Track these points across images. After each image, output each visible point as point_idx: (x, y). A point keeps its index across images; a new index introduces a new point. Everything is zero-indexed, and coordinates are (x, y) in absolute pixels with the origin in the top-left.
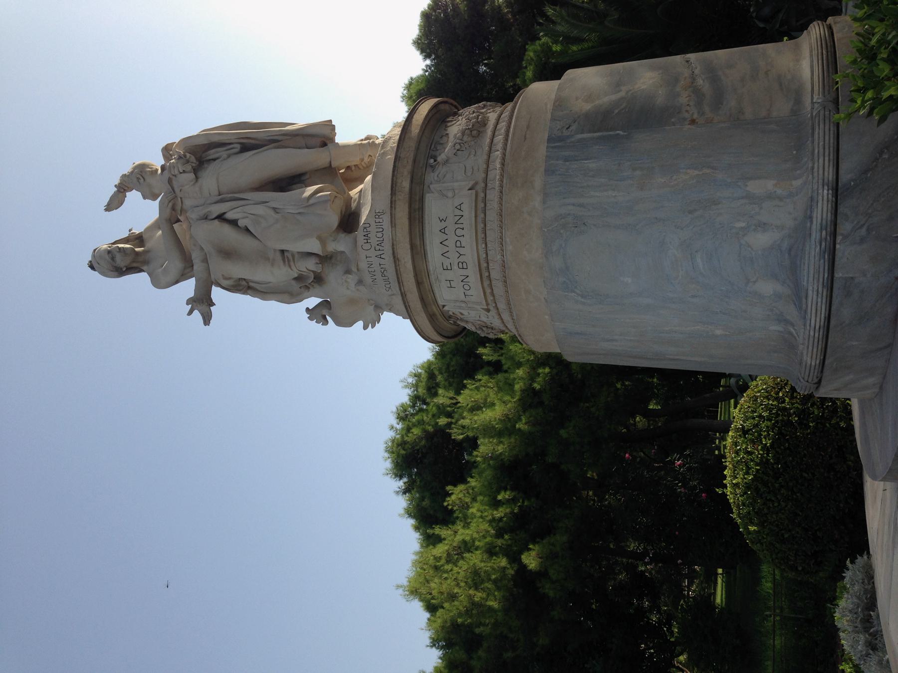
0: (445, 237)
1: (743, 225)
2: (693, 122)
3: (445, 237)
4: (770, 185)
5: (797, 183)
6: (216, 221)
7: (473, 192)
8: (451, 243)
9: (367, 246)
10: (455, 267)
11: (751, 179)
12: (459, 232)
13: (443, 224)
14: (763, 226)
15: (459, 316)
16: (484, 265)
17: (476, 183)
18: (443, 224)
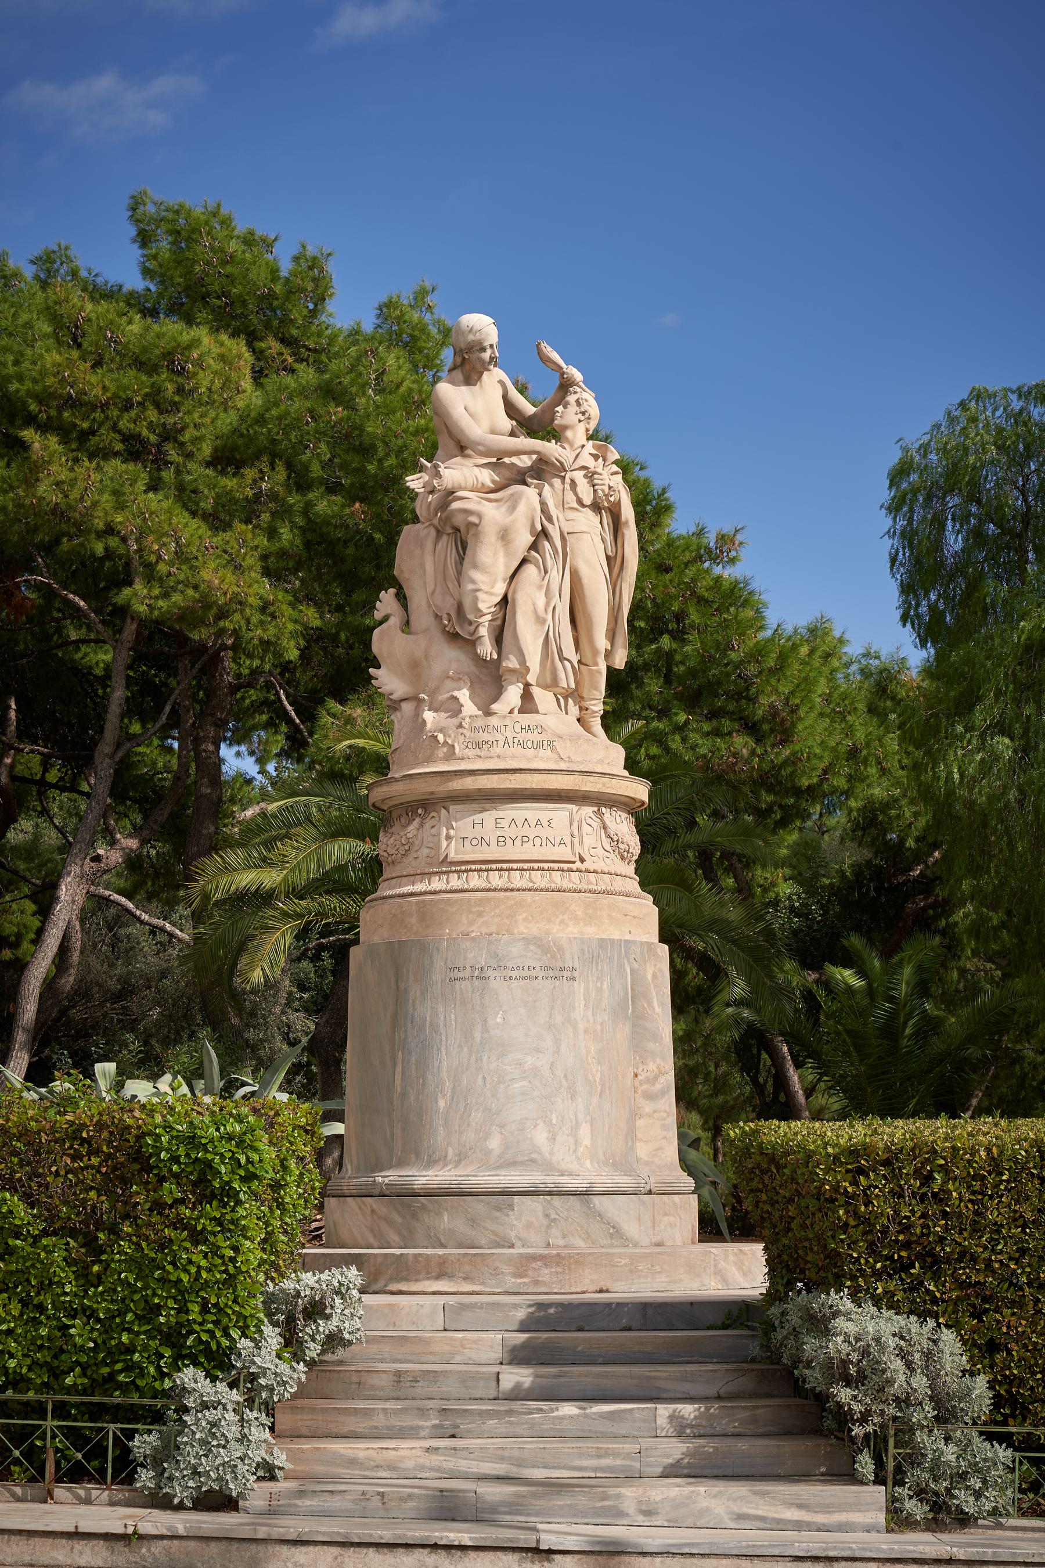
0: (533, 825)
1: (554, 1121)
2: (636, 1076)
3: (533, 825)
4: (587, 1142)
5: (588, 1164)
6: (539, 528)
7: (577, 859)
8: (526, 831)
9: (518, 729)
10: (499, 833)
11: (592, 1125)
12: (538, 841)
13: (545, 824)
14: (553, 1139)
15: (428, 824)
16: (505, 866)
17: (582, 860)
18: (545, 824)
